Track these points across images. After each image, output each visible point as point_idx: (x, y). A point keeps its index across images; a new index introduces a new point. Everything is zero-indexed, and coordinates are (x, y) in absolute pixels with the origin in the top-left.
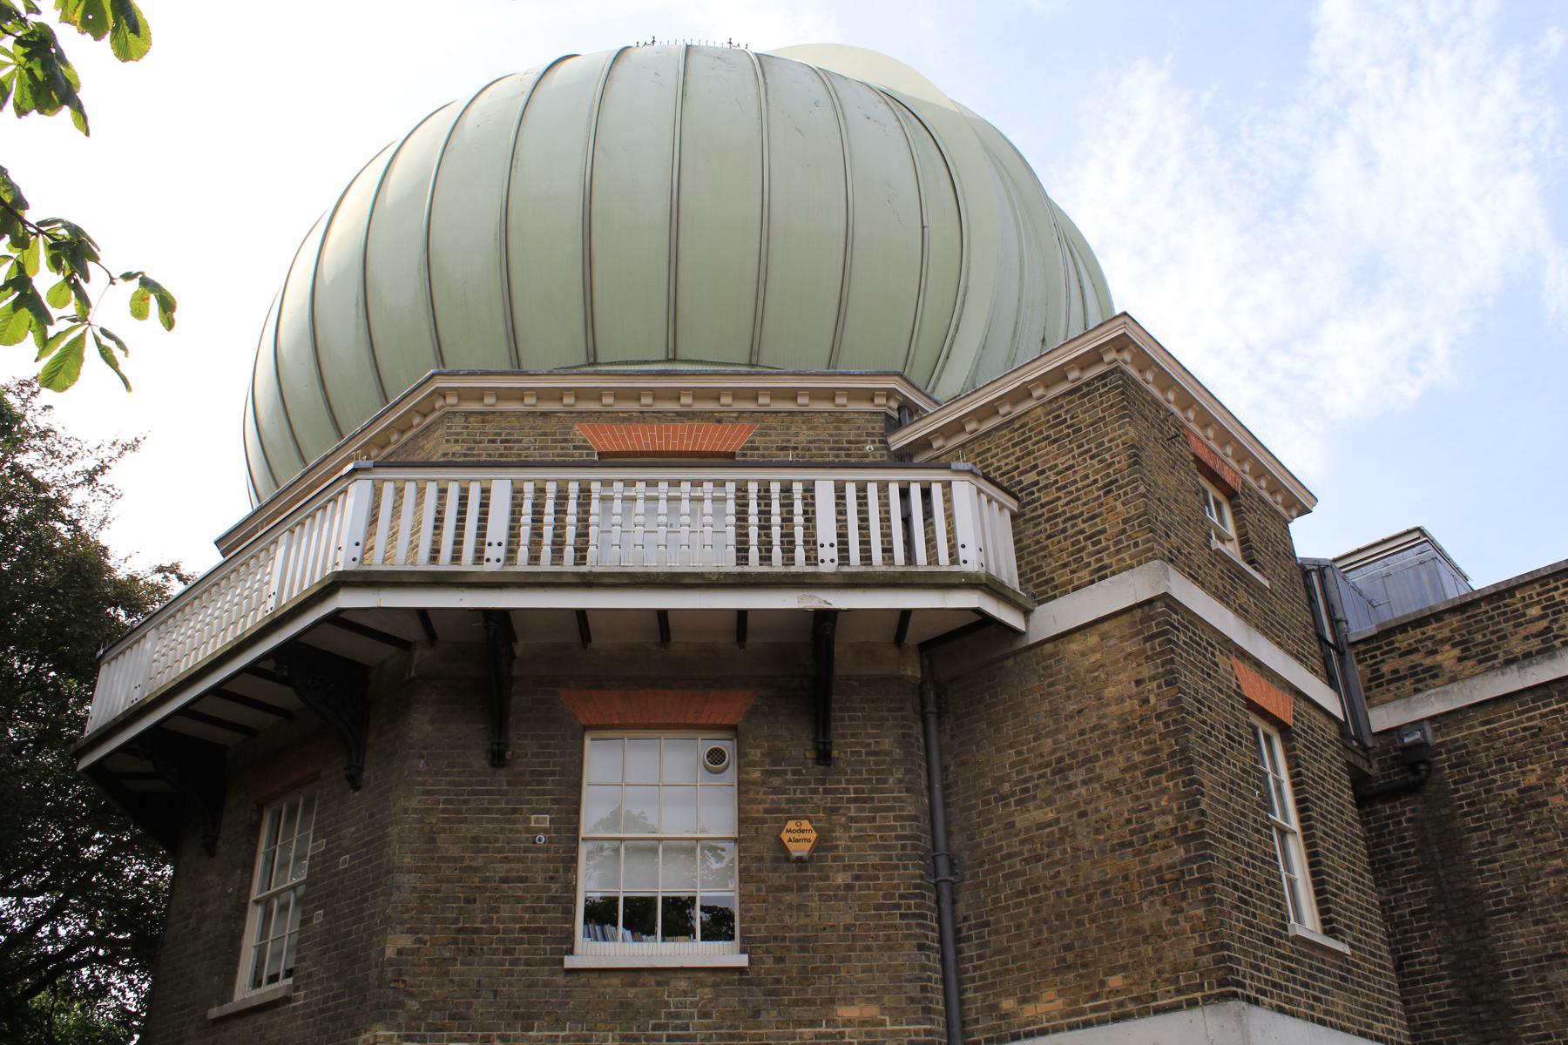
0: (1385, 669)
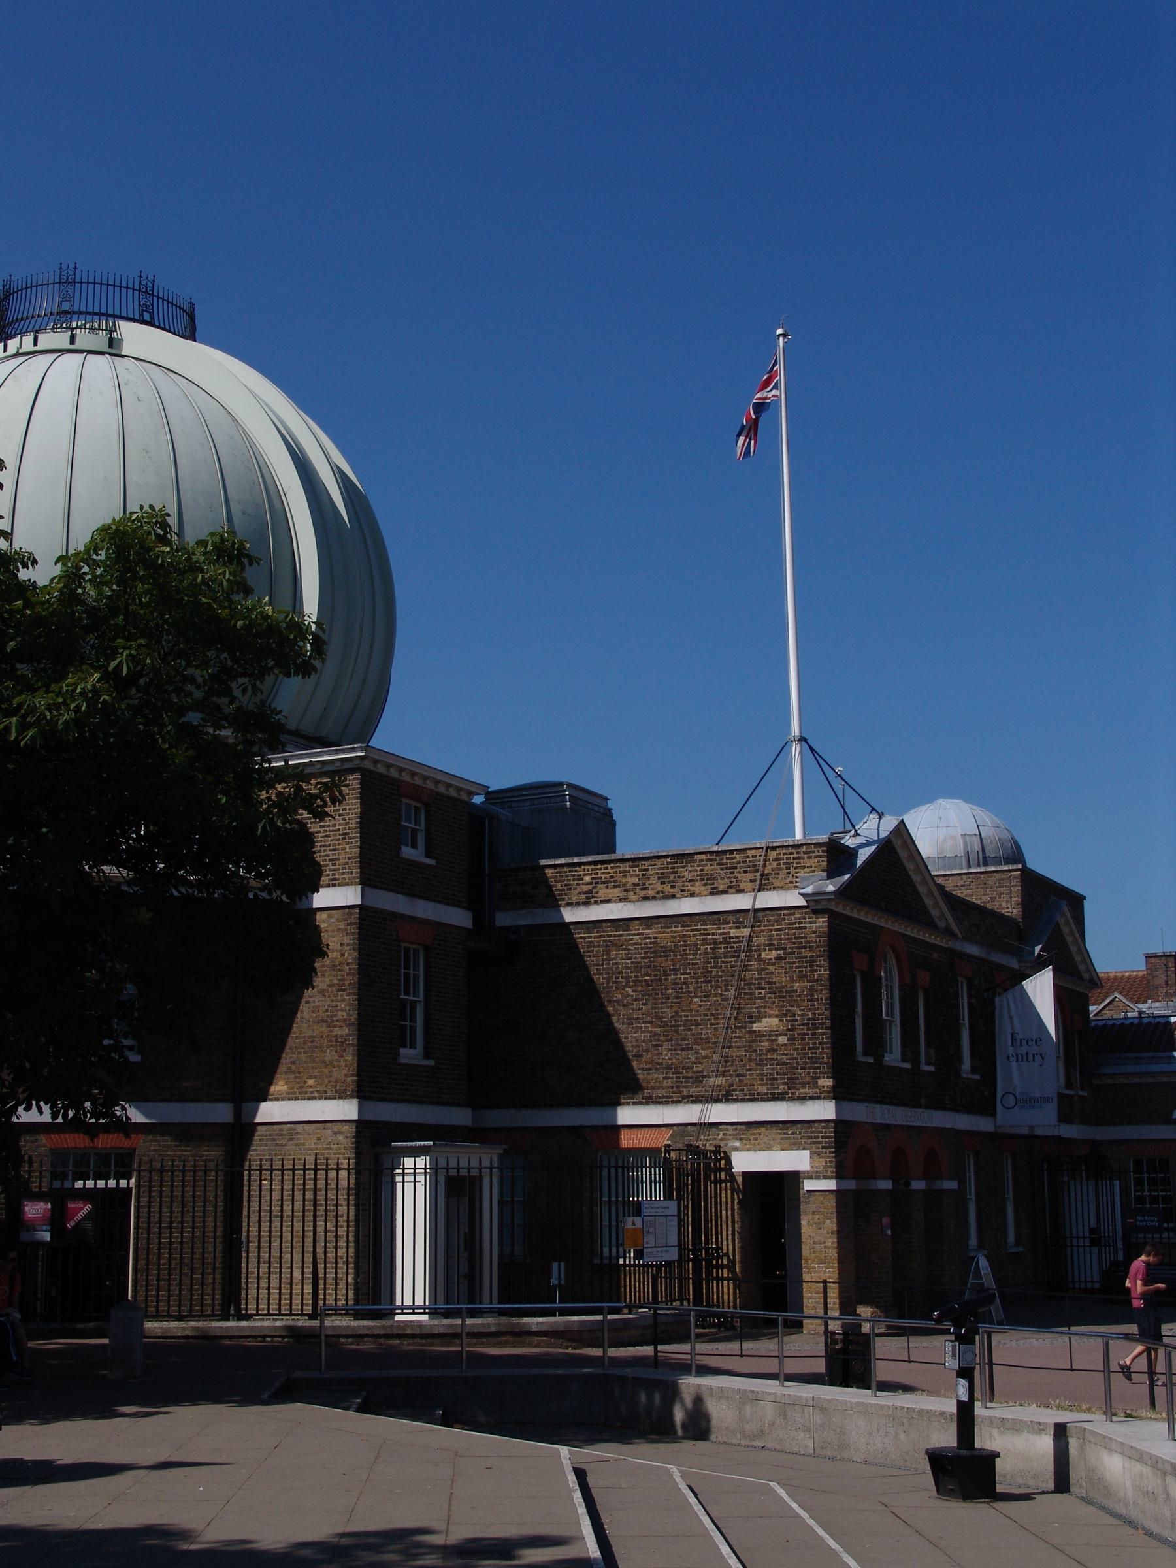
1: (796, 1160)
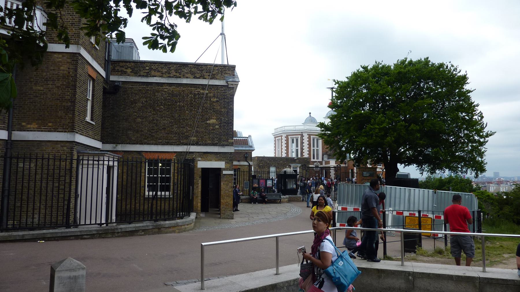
0: (116, 68)
1: (221, 165)
